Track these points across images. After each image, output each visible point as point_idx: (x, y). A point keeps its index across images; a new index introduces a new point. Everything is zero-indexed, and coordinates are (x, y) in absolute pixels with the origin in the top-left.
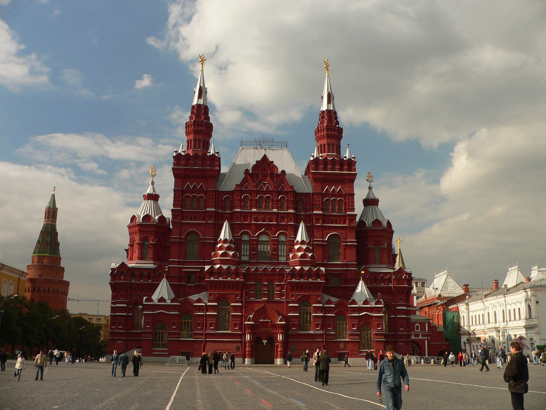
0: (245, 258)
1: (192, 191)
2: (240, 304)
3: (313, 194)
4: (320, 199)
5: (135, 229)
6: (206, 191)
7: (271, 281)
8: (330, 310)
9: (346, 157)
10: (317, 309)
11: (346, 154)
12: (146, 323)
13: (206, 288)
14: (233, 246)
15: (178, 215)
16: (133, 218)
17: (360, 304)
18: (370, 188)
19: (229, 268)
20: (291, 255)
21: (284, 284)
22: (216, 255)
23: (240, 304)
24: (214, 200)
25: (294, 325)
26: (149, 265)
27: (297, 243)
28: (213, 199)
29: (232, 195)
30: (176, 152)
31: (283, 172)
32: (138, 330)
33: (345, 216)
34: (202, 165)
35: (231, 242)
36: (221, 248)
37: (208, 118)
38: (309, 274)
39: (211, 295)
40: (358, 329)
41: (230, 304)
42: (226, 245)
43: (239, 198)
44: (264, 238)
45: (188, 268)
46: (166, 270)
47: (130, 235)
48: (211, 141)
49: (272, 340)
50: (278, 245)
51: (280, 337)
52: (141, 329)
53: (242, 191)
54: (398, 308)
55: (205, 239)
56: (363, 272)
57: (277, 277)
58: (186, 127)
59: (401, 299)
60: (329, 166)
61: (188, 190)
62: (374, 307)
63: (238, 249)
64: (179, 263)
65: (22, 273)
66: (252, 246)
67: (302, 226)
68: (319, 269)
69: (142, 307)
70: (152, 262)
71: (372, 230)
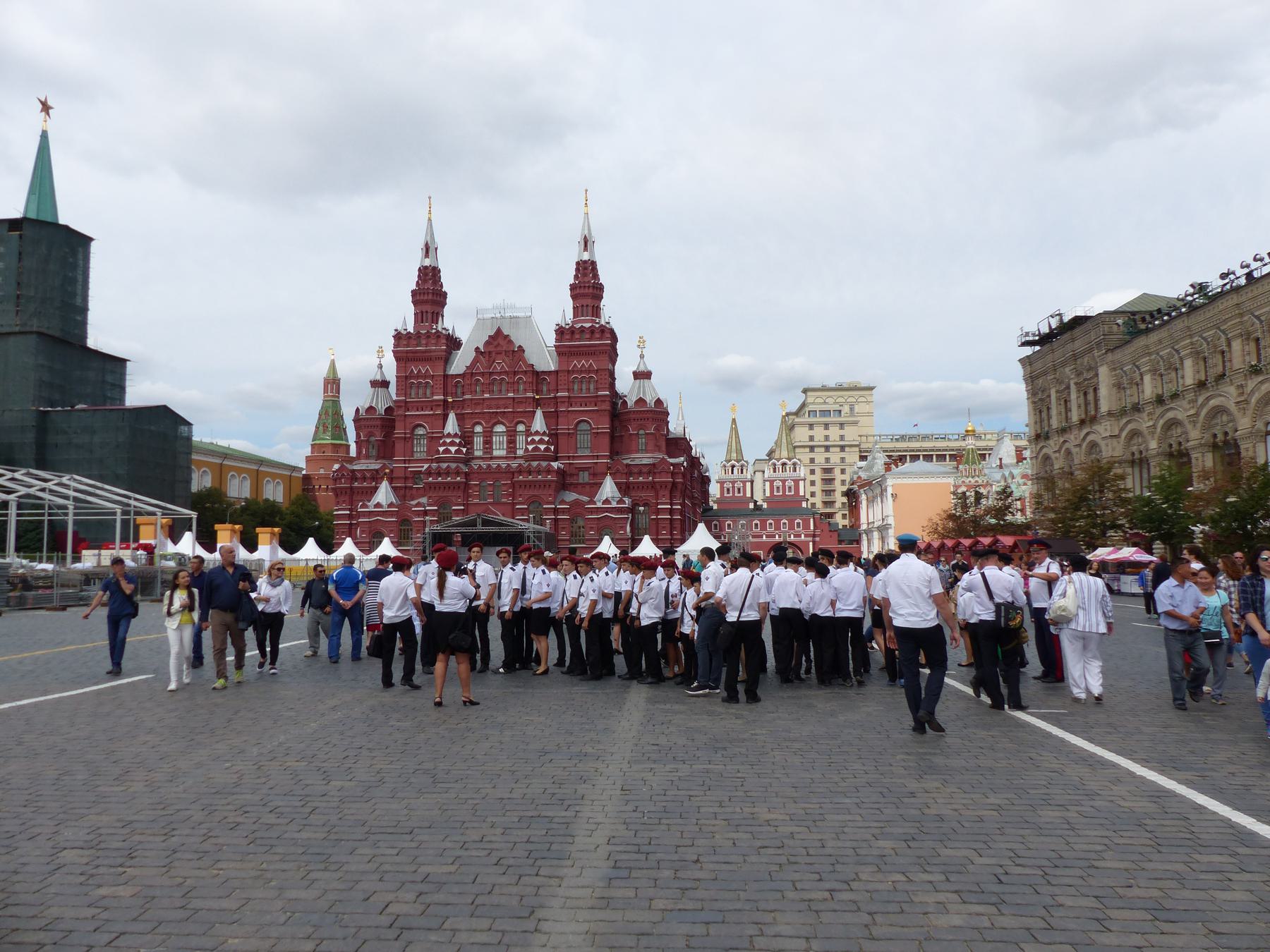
0: (478, 453)
3: (556, 372)
8: (563, 511)
12: (362, 532)
16: (358, 410)
17: (599, 505)
18: (642, 356)
26: (375, 466)
35: (456, 435)
36: (444, 444)
42: (448, 440)
44: (500, 428)
50: (515, 436)
60: (577, 336)
61: (411, 376)
64: (405, 462)
65: (294, 469)
67: (539, 413)
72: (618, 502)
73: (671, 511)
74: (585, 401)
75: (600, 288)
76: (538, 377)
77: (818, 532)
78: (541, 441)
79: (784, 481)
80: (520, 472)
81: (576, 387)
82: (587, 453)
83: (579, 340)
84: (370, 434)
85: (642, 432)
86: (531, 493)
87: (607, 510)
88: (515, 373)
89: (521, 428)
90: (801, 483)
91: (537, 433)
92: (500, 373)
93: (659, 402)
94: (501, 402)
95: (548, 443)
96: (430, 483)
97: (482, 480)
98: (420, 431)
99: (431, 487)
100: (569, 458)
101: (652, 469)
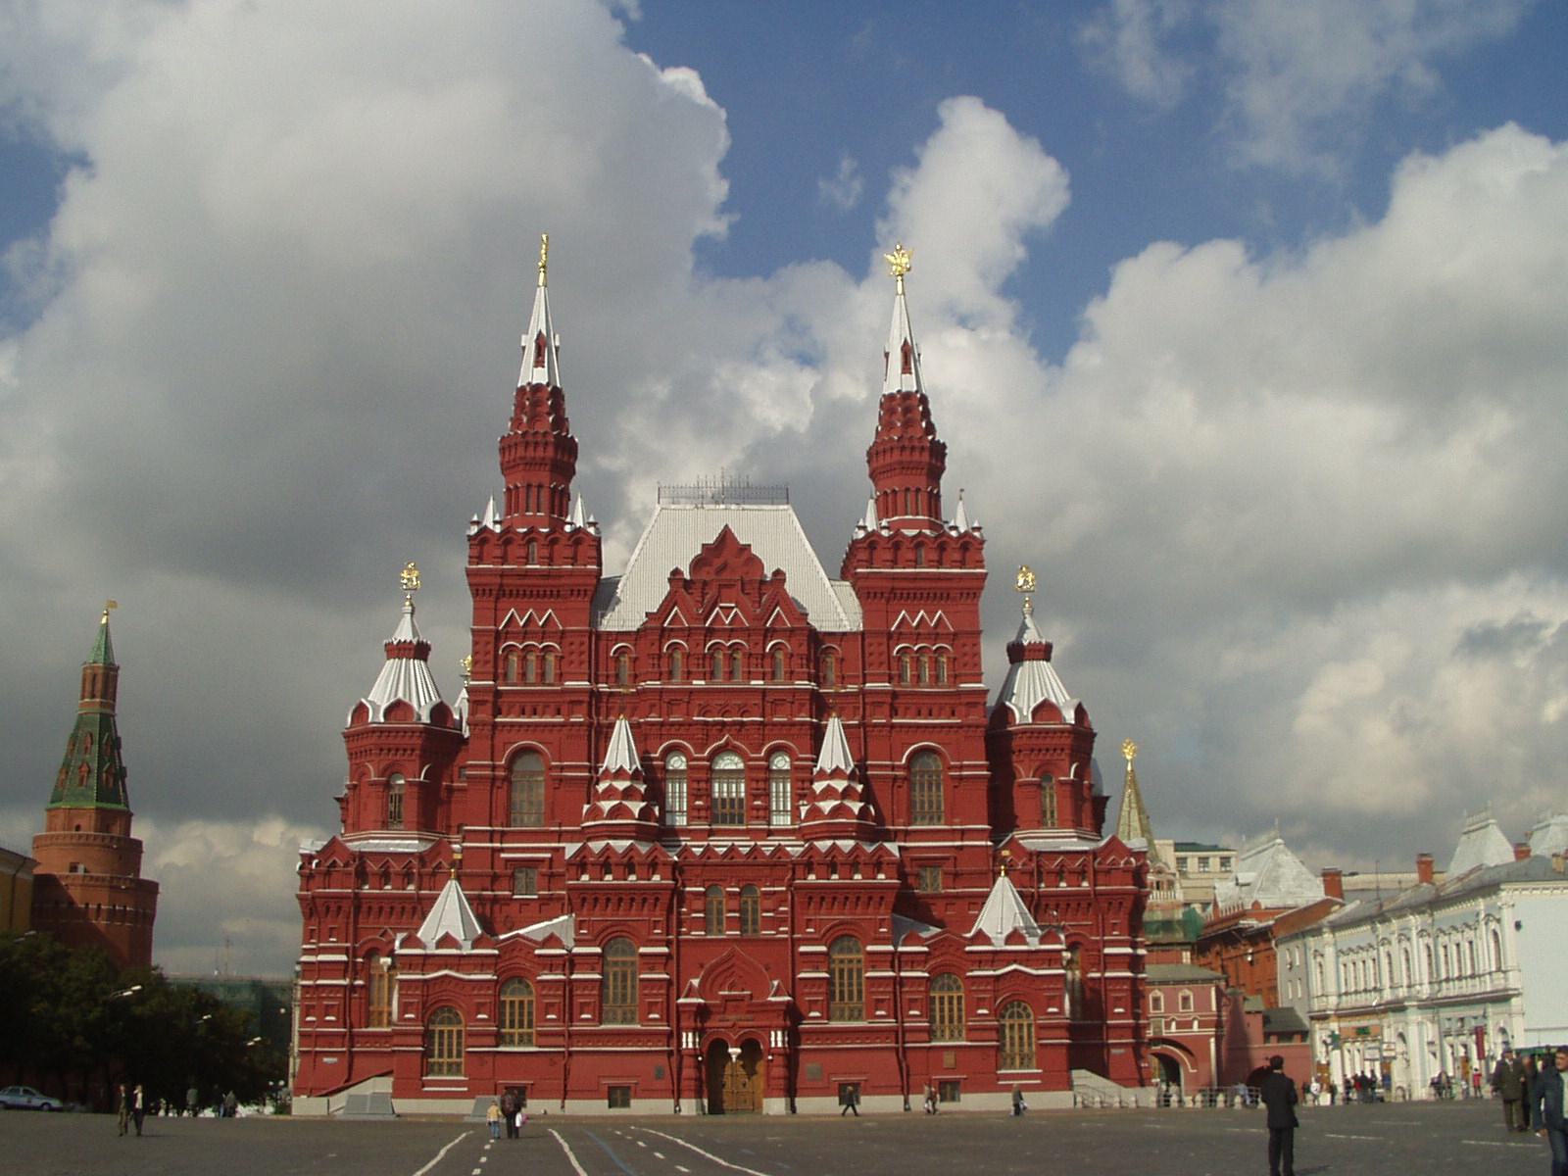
1: (525, 634)
2: (665, 950)
3: (863, 634)
5: (365, 742)
6: (563, 632)
7: (747, 887)
8: (913, 960)
9: (955, 528)
10: (875, 960)
11: (958, 519)
12: (404, 1008)
13: (570, 903)
14: (642, 788)
15: (487, 701)
17: (999, 945)
19: (631, 848)
20: (804, 810)
22: (595, 813)
23: (665, 950)
24: (585, 657)
25: (812, 1006)
26: (409, 844)
27: (822, 775)
28: (582, 653)
29: (635, 645)
30: (478, 523)
31: (778, 573)
32: (380, 1024)
34: (551, 560)
35: (635, 776)
36: (610, 793)
37: (561, 422)
38: (853, 862)
39: (580, 925)
40: (998, 1013)
43: (654, 650)
44: (730, 763)
45: (514, 850)
46: (458, 856)
47: (350, 759)
48: (572, 486)
49: (752, 1049)
50: (767, 780)
52: (390, 1023)
53: (663, 629)
55: (562, 768)
56: (1006, 853)
57: (767, 871)
58: (502, 450)
59: (1114, 926)
64: (491, 836)
66: (695, 785)
68: (881, 848)
69: (389, 960)
70: (414, 833)
71: (1032, 732)
75: (939, 451)
80: (809, 867)
83: (916, 564)
84: (389, 771)
87: (1015, 957)
89: (782, 762)
92: (730, 633)
96: (585, 888)
97: (712, 885)
98: (525, 764)
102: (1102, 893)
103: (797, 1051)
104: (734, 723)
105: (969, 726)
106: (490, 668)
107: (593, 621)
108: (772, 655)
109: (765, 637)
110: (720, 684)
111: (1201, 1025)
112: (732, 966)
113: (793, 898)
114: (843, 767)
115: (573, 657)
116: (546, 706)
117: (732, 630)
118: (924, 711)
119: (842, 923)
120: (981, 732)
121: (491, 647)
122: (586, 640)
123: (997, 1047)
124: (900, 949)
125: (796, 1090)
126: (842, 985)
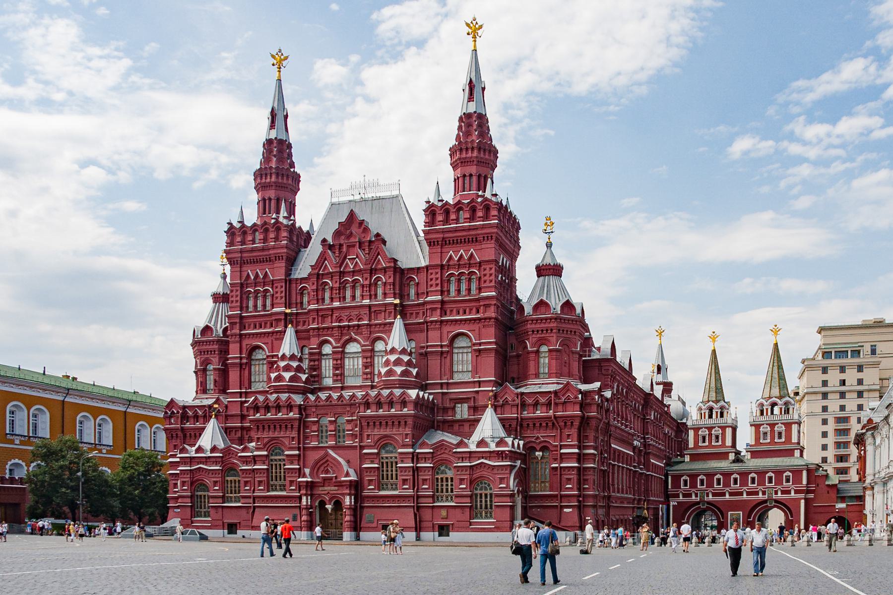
4: (439, 275)
17: (473, 447)
21: (356, 420)
24: (283, 294)
33: (478, 300)
35: (293, 357)
41: (283, 451)
42: (282, 364)
44: (353, 348)
51: (347, 501)
53: (318, 275)
54: (563, 451)
57: (348, 409)
62: (494, 452)
63: (315, 368)
72: (498, 444)
73: (580, 458)
74: (463, 306)
76: (402, 276)
77: (813, 487)
78: (398, 362)
79: (772, 426)
80: (367, 405)
81: (453, 288)
82: (467, 378)
85: (544, 349)
86: (383, 432)
87: (483, 455)
88: (372, 271)
89: (380, 346)
90: (795, 428)
91: (393, 351)
92: (354, 273)
93: (568, 306)
94: (355, 313)
95: (409, 363)
99: (261, 425)
100: (442, 384)
101: (552, 399)
102: (561, 417)
103: (362, 508)
104: (354, 326)
105: (485, 319)
106: (238, 304)
107: (288, 273)
108: (376, 284)
109: (371, 274)
110: (348, 302)
111: (796, 492)
112: (327, 461)
113: (361, 423)
114: (397, 347)
115: (278, 295)
116: (266, 323)
117: (353, 272)
118: (461, 311)
119: (386, 436)
120: (492, 322)
121: (238, 293)
122: (284, 284)
123: (471, 507)
124: (418, 451)
125: (361, 528)
126: (387, 471)
